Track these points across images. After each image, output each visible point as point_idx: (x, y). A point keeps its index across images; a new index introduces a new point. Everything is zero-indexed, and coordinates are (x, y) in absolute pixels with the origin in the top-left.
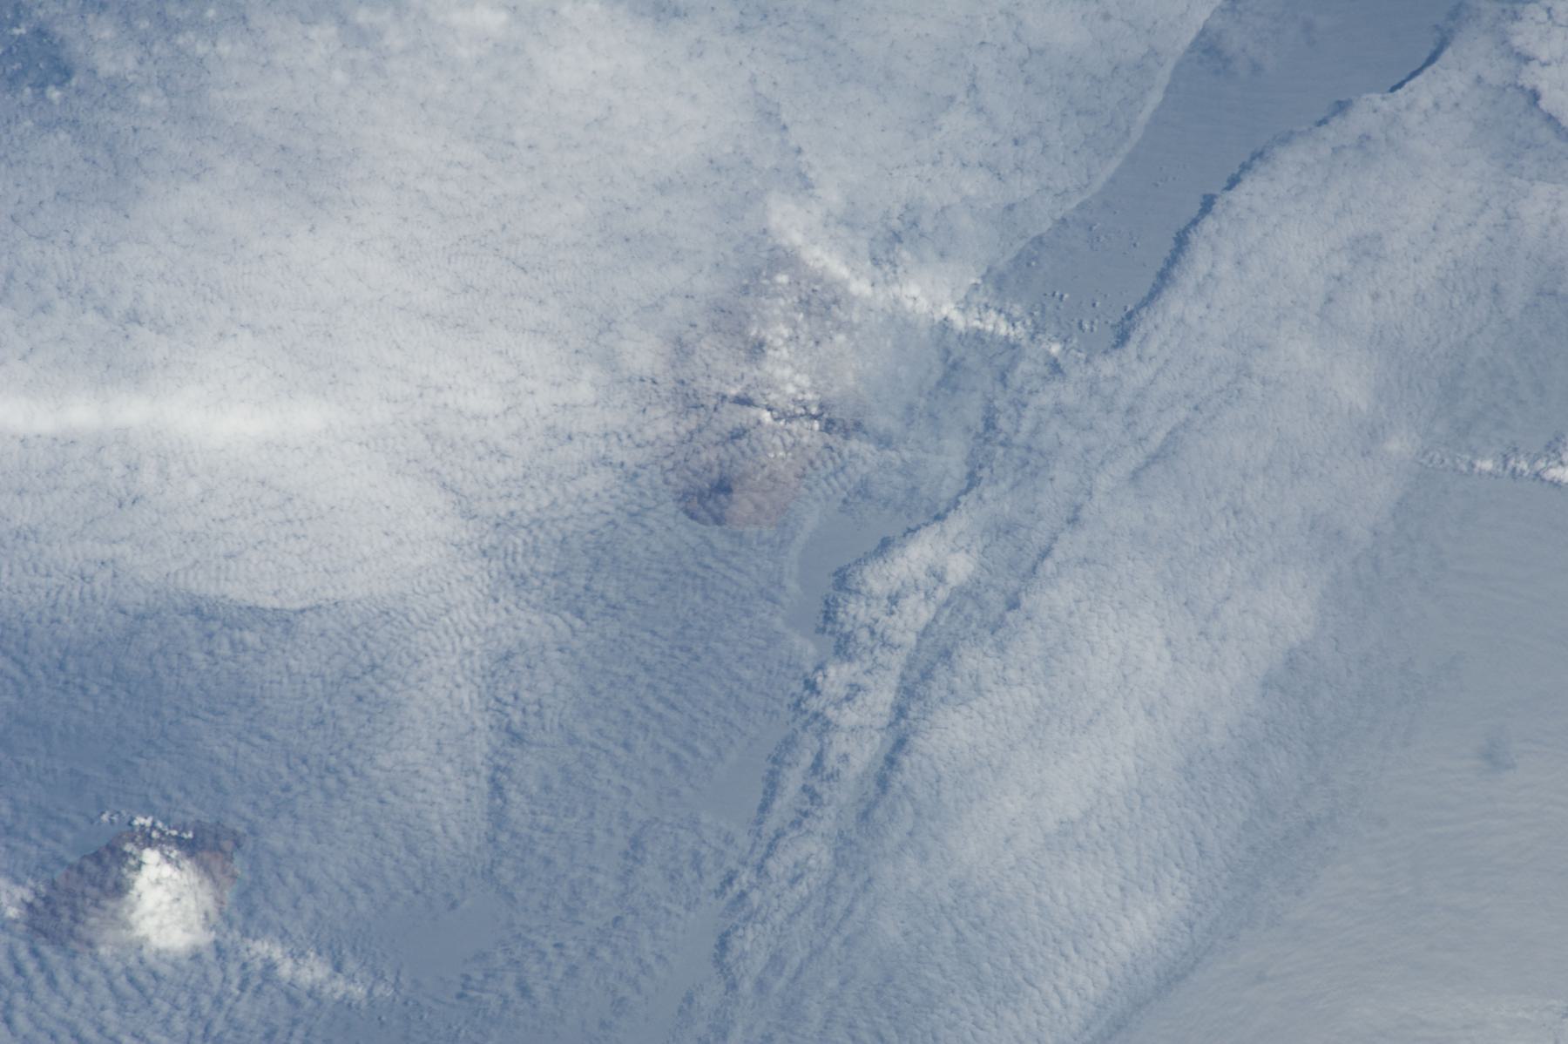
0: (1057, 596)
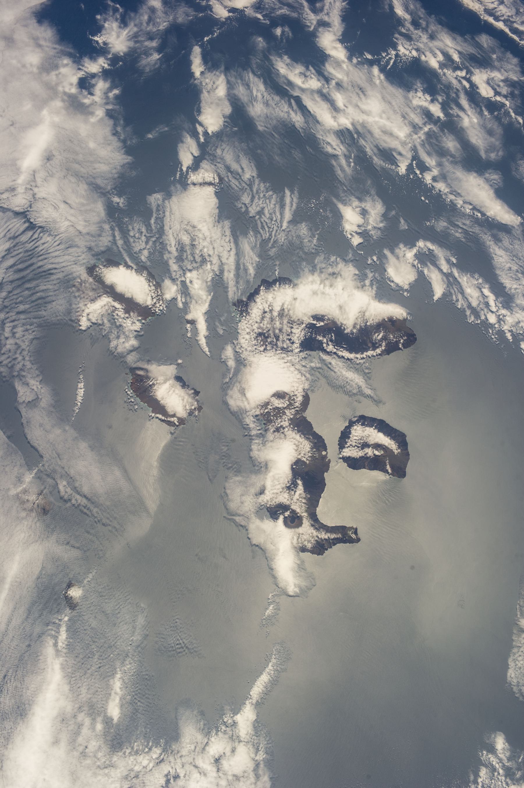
0: (72, 472)
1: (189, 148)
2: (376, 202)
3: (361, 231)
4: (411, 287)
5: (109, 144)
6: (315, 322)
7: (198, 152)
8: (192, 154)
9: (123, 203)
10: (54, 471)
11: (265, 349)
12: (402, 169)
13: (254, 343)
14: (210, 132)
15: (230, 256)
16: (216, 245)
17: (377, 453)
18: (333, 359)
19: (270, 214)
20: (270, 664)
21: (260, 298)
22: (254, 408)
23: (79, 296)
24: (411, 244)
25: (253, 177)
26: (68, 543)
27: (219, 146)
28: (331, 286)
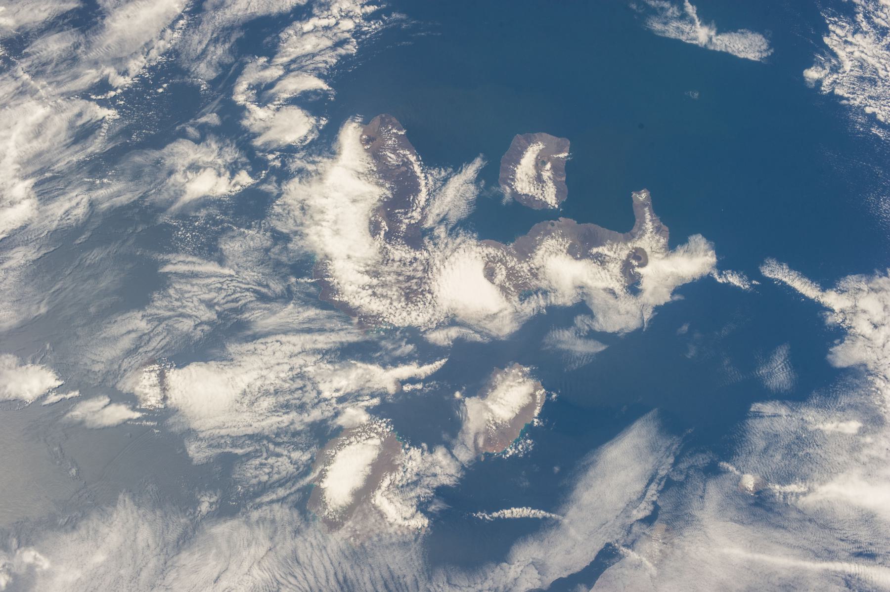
0: (622, 505)
1: (94, 413)
2: (175, 150)
3: (228, 174)
4: (313, 115)
5: (96, 532)
6: (383, 233)
7: (101, 398)
8: (105, 406)
9: (210, 498)
10: (623, 526)
11: (429, 292)
12: (110, 114)
13: (421, 307)
14: (59, 383)
15: (289, 342)
16: (273, 362)
17: (548, 166)
18: (433, 210)
19: (210, 291)
20: (784, 279)
21: (354, 300)
22: (510, 302)
23: (378, 535)
24: (241, 111)
25: (143, 316)
26: (702, 497)
27: (87, 368)
28: (322, 212)
